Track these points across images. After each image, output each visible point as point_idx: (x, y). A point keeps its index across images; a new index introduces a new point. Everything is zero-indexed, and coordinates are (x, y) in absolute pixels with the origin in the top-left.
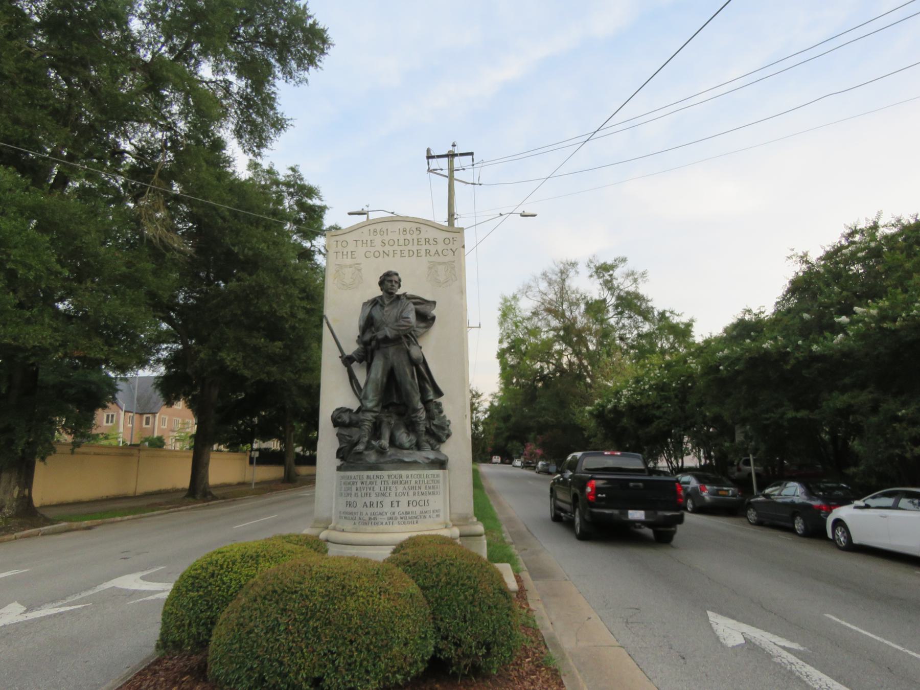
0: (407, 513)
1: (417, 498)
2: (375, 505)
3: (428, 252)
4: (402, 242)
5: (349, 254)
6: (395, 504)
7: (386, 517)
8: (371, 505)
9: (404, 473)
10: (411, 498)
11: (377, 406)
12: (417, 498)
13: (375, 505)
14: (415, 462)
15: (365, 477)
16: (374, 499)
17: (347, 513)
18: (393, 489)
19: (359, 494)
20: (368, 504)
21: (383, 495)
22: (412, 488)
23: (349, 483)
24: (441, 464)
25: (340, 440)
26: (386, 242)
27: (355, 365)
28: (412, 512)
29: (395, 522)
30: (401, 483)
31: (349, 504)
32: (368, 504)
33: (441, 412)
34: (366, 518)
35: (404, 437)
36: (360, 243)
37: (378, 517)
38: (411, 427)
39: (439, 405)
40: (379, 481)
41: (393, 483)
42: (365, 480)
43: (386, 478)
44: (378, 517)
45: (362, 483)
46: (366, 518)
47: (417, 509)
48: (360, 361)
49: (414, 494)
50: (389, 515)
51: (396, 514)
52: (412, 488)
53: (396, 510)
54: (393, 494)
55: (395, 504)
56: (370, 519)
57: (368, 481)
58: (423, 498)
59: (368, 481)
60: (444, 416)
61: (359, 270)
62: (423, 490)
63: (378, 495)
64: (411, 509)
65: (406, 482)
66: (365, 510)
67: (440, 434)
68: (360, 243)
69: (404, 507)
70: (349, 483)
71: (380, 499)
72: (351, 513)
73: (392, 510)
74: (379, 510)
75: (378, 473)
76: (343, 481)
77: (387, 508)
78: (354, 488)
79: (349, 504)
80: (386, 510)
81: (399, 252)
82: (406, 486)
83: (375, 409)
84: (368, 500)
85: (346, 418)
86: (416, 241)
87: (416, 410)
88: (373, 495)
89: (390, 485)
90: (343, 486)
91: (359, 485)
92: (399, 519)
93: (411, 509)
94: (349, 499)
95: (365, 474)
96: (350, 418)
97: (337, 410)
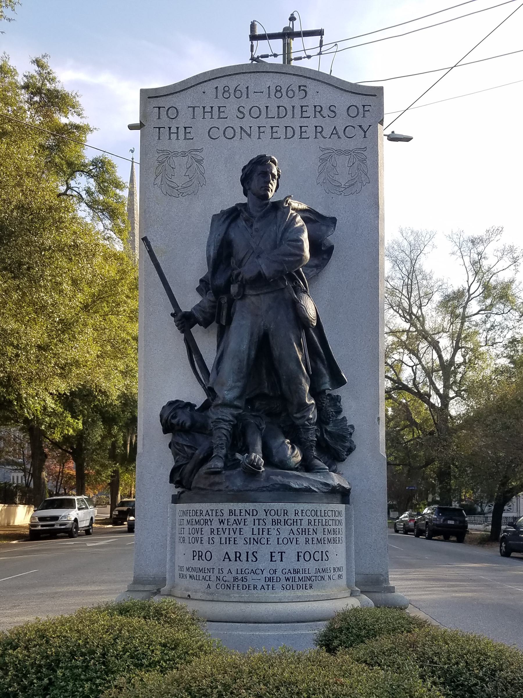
0: (296, 571)
1: (311, 548)
2: (244, 557)
3: (318, 131)
4: (273, 112)
5: (182, 131)
6: (277, 557)
8: (238, 557)
10: (303, 547)
11: (239, 398)
13: (244, 557)
14: (308, 490)
15: (226, 512)
16: (242, 548)
18: (274, 532)
20: (232, 557)
22: (304, 531)
23: (198, 522)
25: (175, 454)
26: (246, 111)
27: (197, 331)
29: (277, 585)
30: (286, 522)
31: (199, 555)
32: (232, 557)
33: (339, 411)
34: (229, 578)
36: (199, 111)
39: (336, 400)
40: (250, 519)
42: (226, 516)
43: (262, 515)
44: (249, 577)
45: (221, 522)
46: (229, 578)
47: (312, 566)
48: (206, 324)
49: (307, 542)
50: (266, 574)
51: (279, 574)
52: (304, 531)
53: (280, 566)
54: (273, 540)
55: (277, 557)
56: (235, 579)
58: (320, 547)
61: (199, 162)
62: (320, 535)
64: (301, 565)
65: (295, 522)
68: (199, 111)
69: (290, 562)
70: (198, 522)
71: (252, 548)
73: (273, 566)
75: (249, 506)
76: (186, 518)
77: (264, 563)
78: (206, 529)
79: (199, 555)
82: (295, 528)
84: (231, 549)
85: (184, 418)
86: (298, 111)
87: (303, 407)
88: (240, 542)
90: (187, 527)
91: (216, 525)
93: (301, 565)
94: (198, 547)
96: (192, 418)
97: (171, 404)
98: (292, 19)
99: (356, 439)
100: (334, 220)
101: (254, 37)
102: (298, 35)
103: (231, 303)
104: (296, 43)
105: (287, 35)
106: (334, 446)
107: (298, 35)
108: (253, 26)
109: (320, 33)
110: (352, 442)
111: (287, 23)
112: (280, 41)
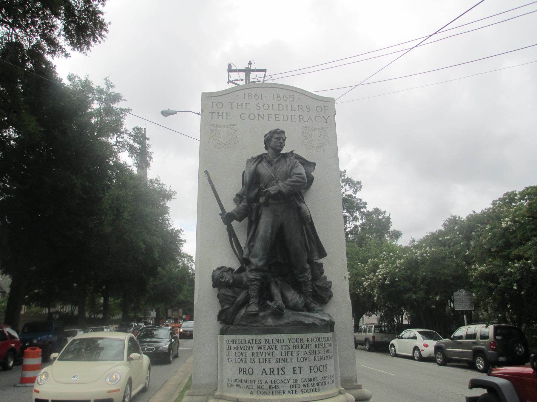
0: (310, 380)
1: (318, 363)
2: (276, 372)
3: (301, 118)
4: (276, 107)
5: (225, 115)
6: (298, 371)
7: (288, 385)
8: (272, 372)
9: (304, 336)
10: (313, 363)
11: (265, 265)
12: (318, 363)
13: (276, 372)
14: (314, 324)
15: (263, 341)
16: (274, 365)
17: (239, 381)
18: (295, 354)
19: (256, 359)
20: (268, 371)
21: (285, 361)
22: (313, 352)
23: (243, 348)
24: (329, 326)
25: (222, 302)
26: (261, 106)
28: (314, 379)
29: (299, 390)
30: (302, 347)
31: (244, 371)
32: (268, 371)
33: (322, 272)
34: (266, 386)
35: (293, 296)
36: (235, 105)
37: (280, 385)
38: (298, 286)
39: (321, 265)
40: (279, 345)
41: (295, 347)
42: (263, 344)
43: (286, 342)
44: (280, 385)
45: (260, 348)
46: (266, 386)
47: (318, 375)
48: (240, 220)
49: (315, 359)
50: (291, 383)
51: (299, 382)
52: (313, 352)
53: (299, 377)
54: (295, 360)
55: (298, 371)
56: (270, 387)
57: (267, 345)
58: (323, 362)
59: (267, 345)
60: (325, 277)
61: (235, 131)
62: (322, 354)
63: (278, 361)
64: (313, 375)
65: (307, 346)
66: (263, 377)
67: (324, 295)
68: (235, 105)
69: (306, 374)
70: (243, 348)
71: (282, 365)
72: (245, 381)
73: (295, 377)
74: (280, 377)
75: (278, 336)
76: (232, 345)
77: (289, 375)
78: (249, 352)
79: (244, 371)
80: (287, 378)
81: (274, 116)
82: (307, 350)
83: (264, 268)
84: (267, 366)
85: (228, 277)
86: (289, 107)
87: (304, 270)
88: (273, 361)
89: (292, 350)
90: (234, 352)
91: (255, 350)
92: (302, 388)
93: (313, 375)
94: (243, 365)
95: (263, 337)
96: (233, 277)
97: (219, 269)
98: (250, 63)
99: (333, 290)
100: (314, 164)
101: (230, 70)
102: (254, 71)
103: (258, 208)
104: (253, 75)
105: (248, 71)
106: (321, 295)
107: (254, 71)
108: (230, 65)
109: (265, 71)
110: (331, 292)
111: (247, 65)
112: (244, 74)
